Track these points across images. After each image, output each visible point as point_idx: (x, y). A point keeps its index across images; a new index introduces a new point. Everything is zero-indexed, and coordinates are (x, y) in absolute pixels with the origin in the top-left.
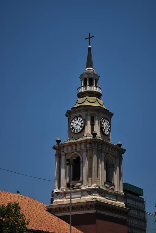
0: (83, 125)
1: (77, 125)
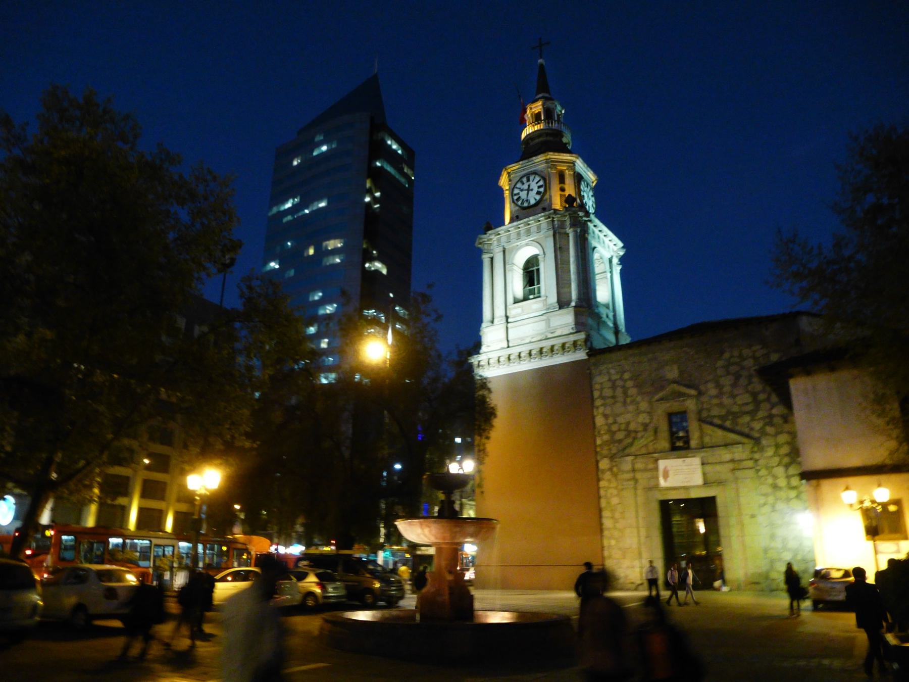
0: (542, 190)
1: (529, 190)
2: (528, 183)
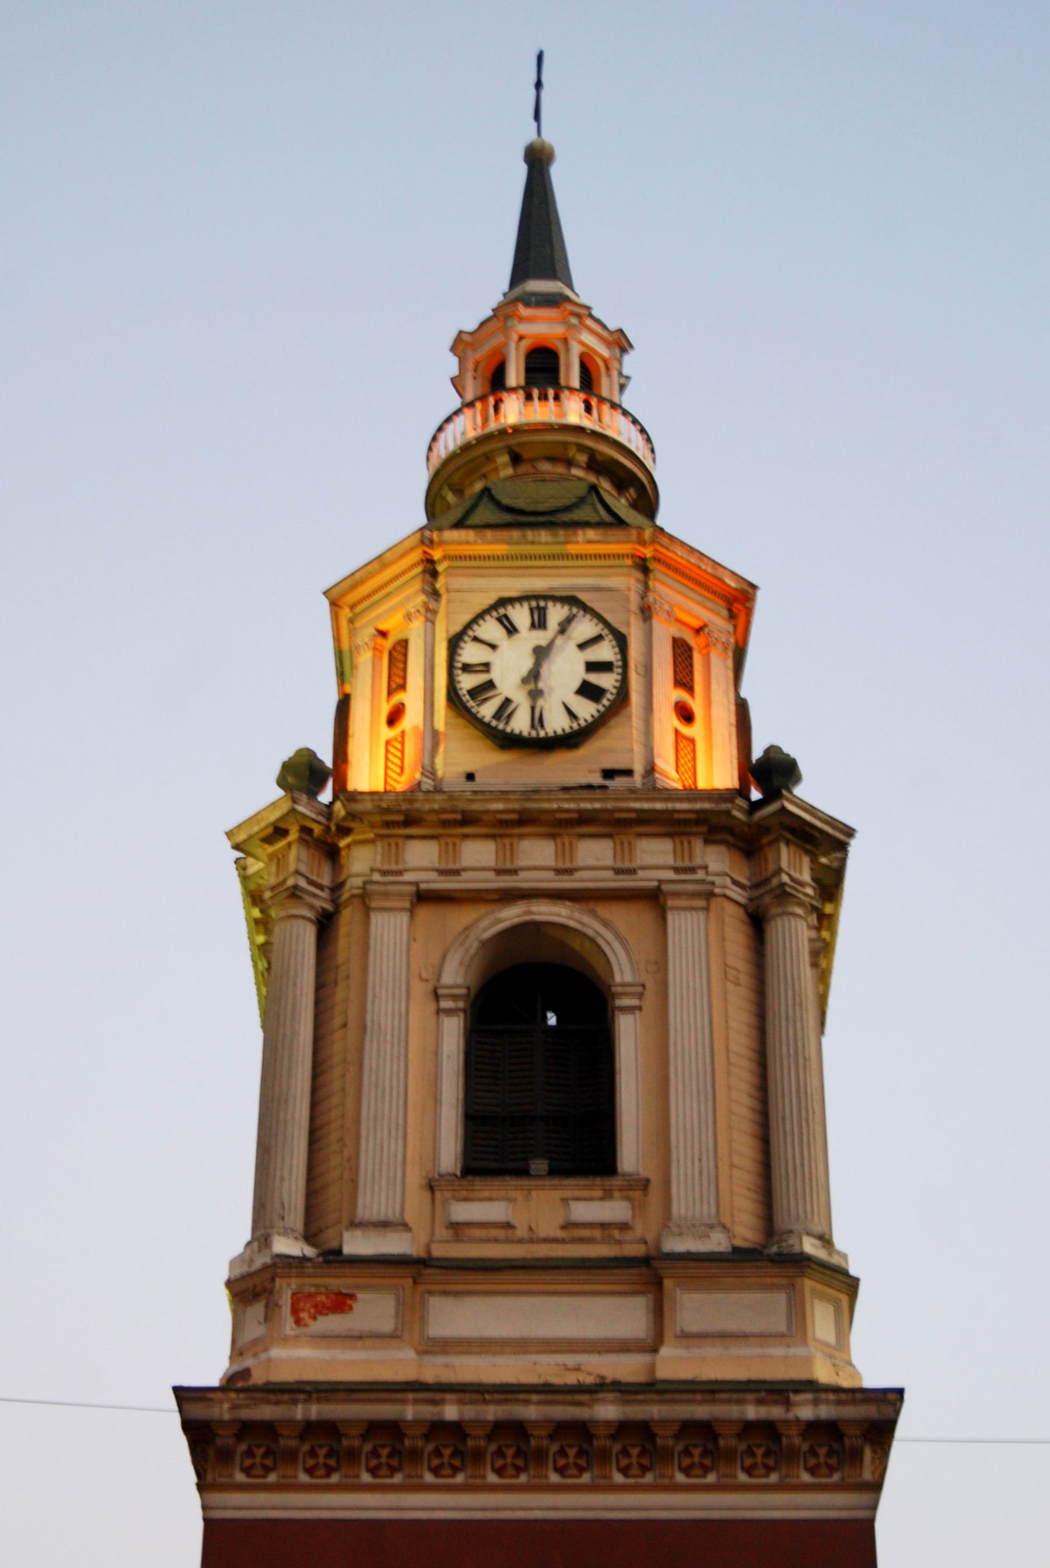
2: (541, 638)
